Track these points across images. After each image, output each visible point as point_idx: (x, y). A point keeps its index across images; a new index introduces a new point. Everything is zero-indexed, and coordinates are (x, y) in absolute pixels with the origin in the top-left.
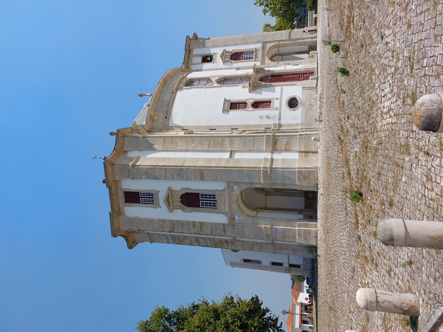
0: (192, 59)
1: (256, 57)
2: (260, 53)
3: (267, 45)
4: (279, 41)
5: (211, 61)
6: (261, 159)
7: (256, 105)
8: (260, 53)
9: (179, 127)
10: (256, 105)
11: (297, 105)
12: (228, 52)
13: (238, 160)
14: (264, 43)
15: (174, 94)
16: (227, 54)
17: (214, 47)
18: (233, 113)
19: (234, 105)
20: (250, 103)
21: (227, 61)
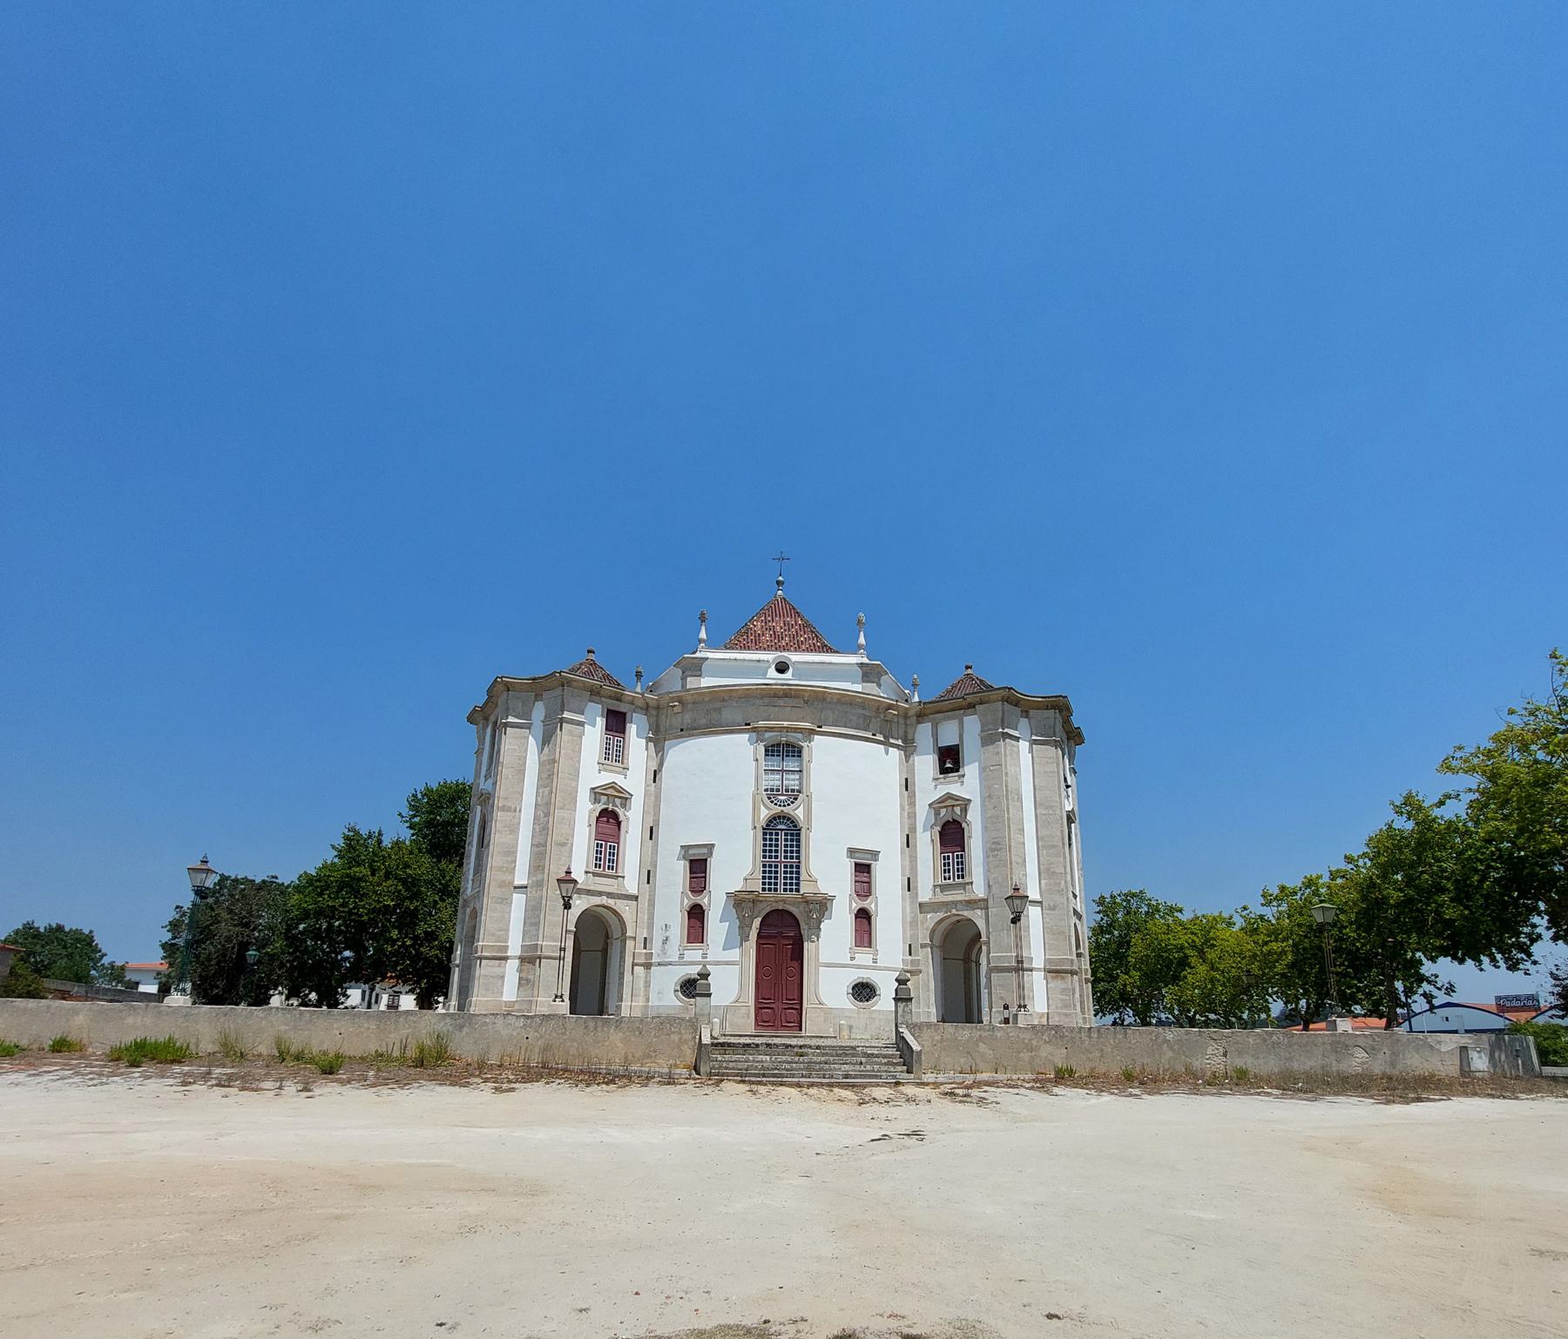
0: (949, 718)
1: (943, 888)
2: (959, 896)
3: (979, 912)
4: (988, 943)
5: (944, 771)
6: (506, 941)
7: (696, 914)
8: (959, 896)
9: (661, 764)
10: (696, 914)
11: (687, 996)
12: (965, 810)
13: (506, 901)
14: (982, 904)
15: (747, 726)
16: (958, 810)
17: (983, 769)
18: (682, 868)
19: (698, 868)
20: (704, 901)
21: (937, 814)
